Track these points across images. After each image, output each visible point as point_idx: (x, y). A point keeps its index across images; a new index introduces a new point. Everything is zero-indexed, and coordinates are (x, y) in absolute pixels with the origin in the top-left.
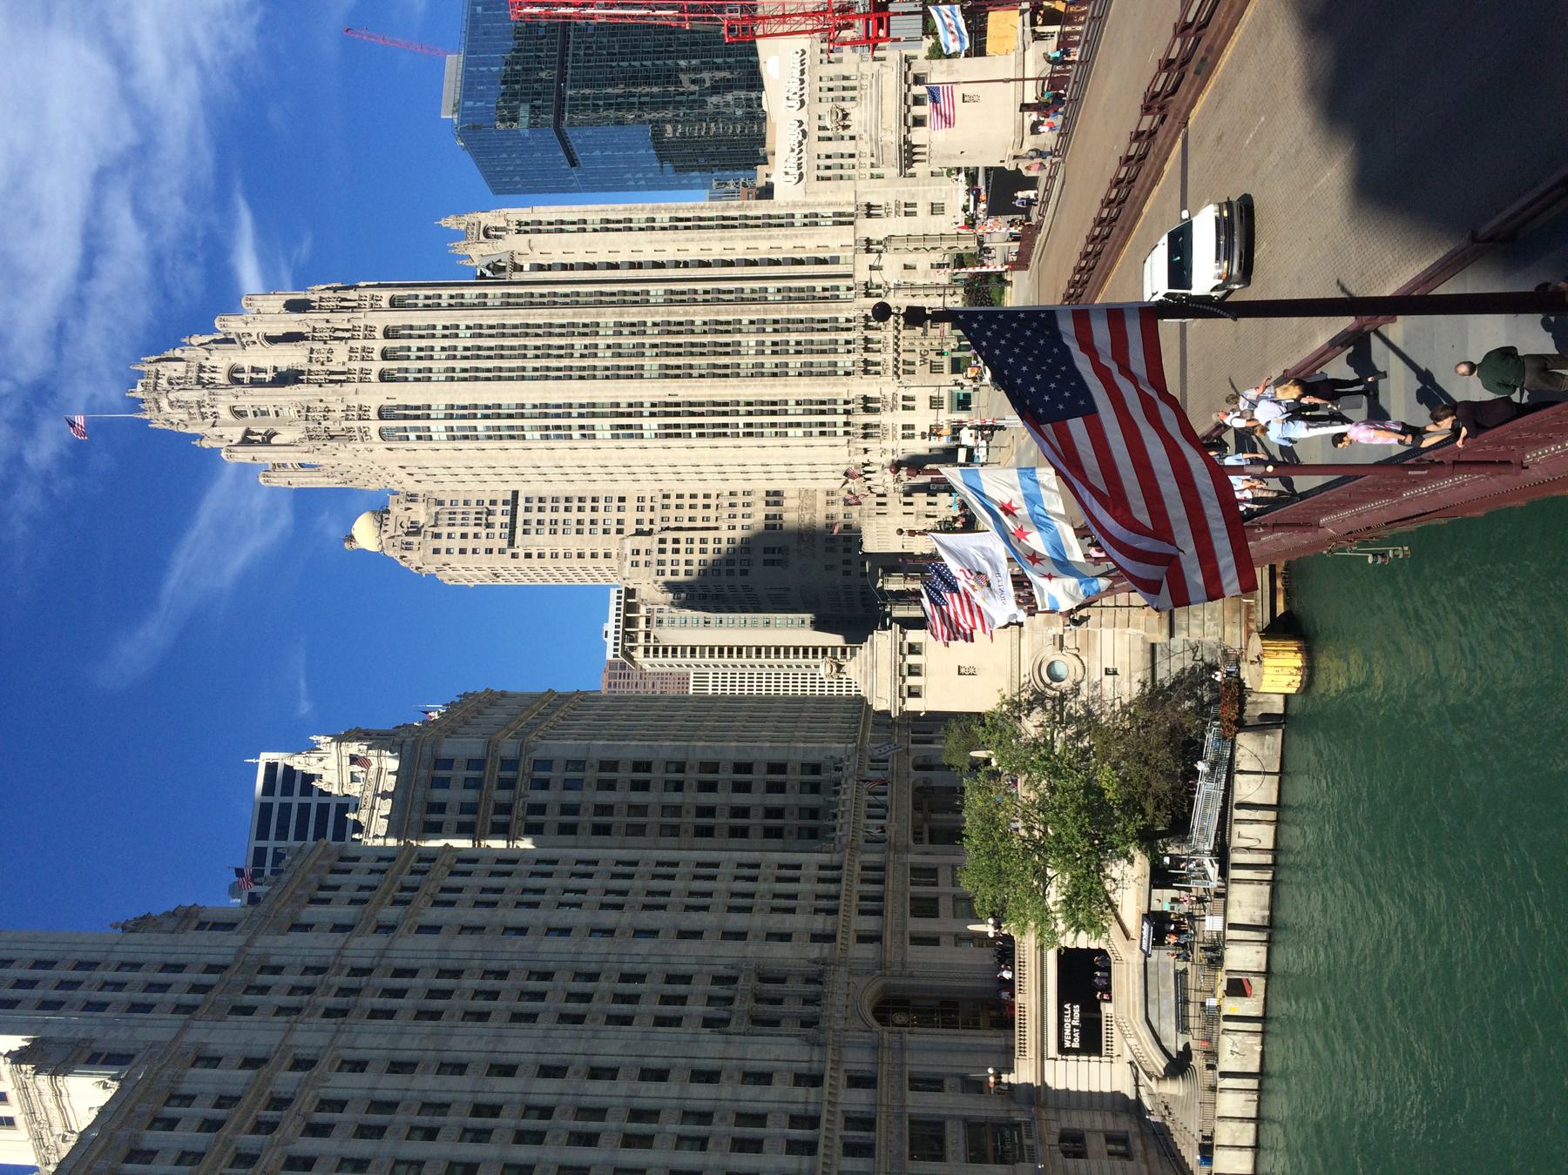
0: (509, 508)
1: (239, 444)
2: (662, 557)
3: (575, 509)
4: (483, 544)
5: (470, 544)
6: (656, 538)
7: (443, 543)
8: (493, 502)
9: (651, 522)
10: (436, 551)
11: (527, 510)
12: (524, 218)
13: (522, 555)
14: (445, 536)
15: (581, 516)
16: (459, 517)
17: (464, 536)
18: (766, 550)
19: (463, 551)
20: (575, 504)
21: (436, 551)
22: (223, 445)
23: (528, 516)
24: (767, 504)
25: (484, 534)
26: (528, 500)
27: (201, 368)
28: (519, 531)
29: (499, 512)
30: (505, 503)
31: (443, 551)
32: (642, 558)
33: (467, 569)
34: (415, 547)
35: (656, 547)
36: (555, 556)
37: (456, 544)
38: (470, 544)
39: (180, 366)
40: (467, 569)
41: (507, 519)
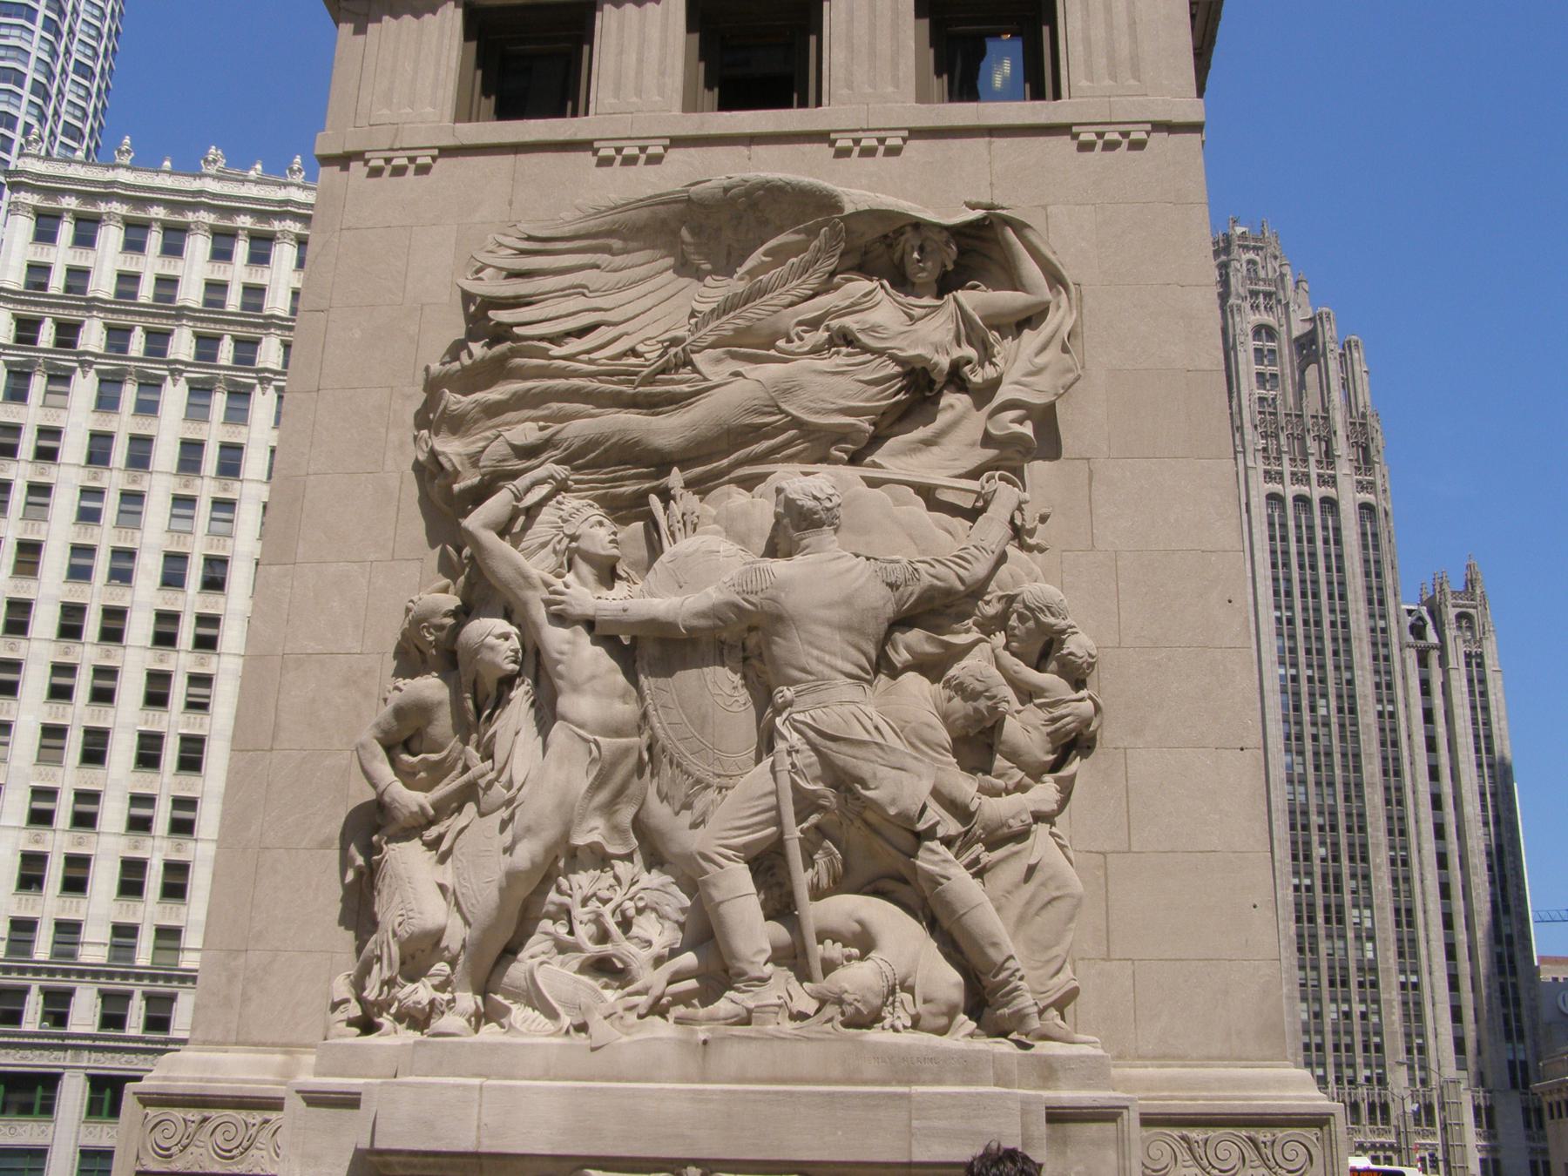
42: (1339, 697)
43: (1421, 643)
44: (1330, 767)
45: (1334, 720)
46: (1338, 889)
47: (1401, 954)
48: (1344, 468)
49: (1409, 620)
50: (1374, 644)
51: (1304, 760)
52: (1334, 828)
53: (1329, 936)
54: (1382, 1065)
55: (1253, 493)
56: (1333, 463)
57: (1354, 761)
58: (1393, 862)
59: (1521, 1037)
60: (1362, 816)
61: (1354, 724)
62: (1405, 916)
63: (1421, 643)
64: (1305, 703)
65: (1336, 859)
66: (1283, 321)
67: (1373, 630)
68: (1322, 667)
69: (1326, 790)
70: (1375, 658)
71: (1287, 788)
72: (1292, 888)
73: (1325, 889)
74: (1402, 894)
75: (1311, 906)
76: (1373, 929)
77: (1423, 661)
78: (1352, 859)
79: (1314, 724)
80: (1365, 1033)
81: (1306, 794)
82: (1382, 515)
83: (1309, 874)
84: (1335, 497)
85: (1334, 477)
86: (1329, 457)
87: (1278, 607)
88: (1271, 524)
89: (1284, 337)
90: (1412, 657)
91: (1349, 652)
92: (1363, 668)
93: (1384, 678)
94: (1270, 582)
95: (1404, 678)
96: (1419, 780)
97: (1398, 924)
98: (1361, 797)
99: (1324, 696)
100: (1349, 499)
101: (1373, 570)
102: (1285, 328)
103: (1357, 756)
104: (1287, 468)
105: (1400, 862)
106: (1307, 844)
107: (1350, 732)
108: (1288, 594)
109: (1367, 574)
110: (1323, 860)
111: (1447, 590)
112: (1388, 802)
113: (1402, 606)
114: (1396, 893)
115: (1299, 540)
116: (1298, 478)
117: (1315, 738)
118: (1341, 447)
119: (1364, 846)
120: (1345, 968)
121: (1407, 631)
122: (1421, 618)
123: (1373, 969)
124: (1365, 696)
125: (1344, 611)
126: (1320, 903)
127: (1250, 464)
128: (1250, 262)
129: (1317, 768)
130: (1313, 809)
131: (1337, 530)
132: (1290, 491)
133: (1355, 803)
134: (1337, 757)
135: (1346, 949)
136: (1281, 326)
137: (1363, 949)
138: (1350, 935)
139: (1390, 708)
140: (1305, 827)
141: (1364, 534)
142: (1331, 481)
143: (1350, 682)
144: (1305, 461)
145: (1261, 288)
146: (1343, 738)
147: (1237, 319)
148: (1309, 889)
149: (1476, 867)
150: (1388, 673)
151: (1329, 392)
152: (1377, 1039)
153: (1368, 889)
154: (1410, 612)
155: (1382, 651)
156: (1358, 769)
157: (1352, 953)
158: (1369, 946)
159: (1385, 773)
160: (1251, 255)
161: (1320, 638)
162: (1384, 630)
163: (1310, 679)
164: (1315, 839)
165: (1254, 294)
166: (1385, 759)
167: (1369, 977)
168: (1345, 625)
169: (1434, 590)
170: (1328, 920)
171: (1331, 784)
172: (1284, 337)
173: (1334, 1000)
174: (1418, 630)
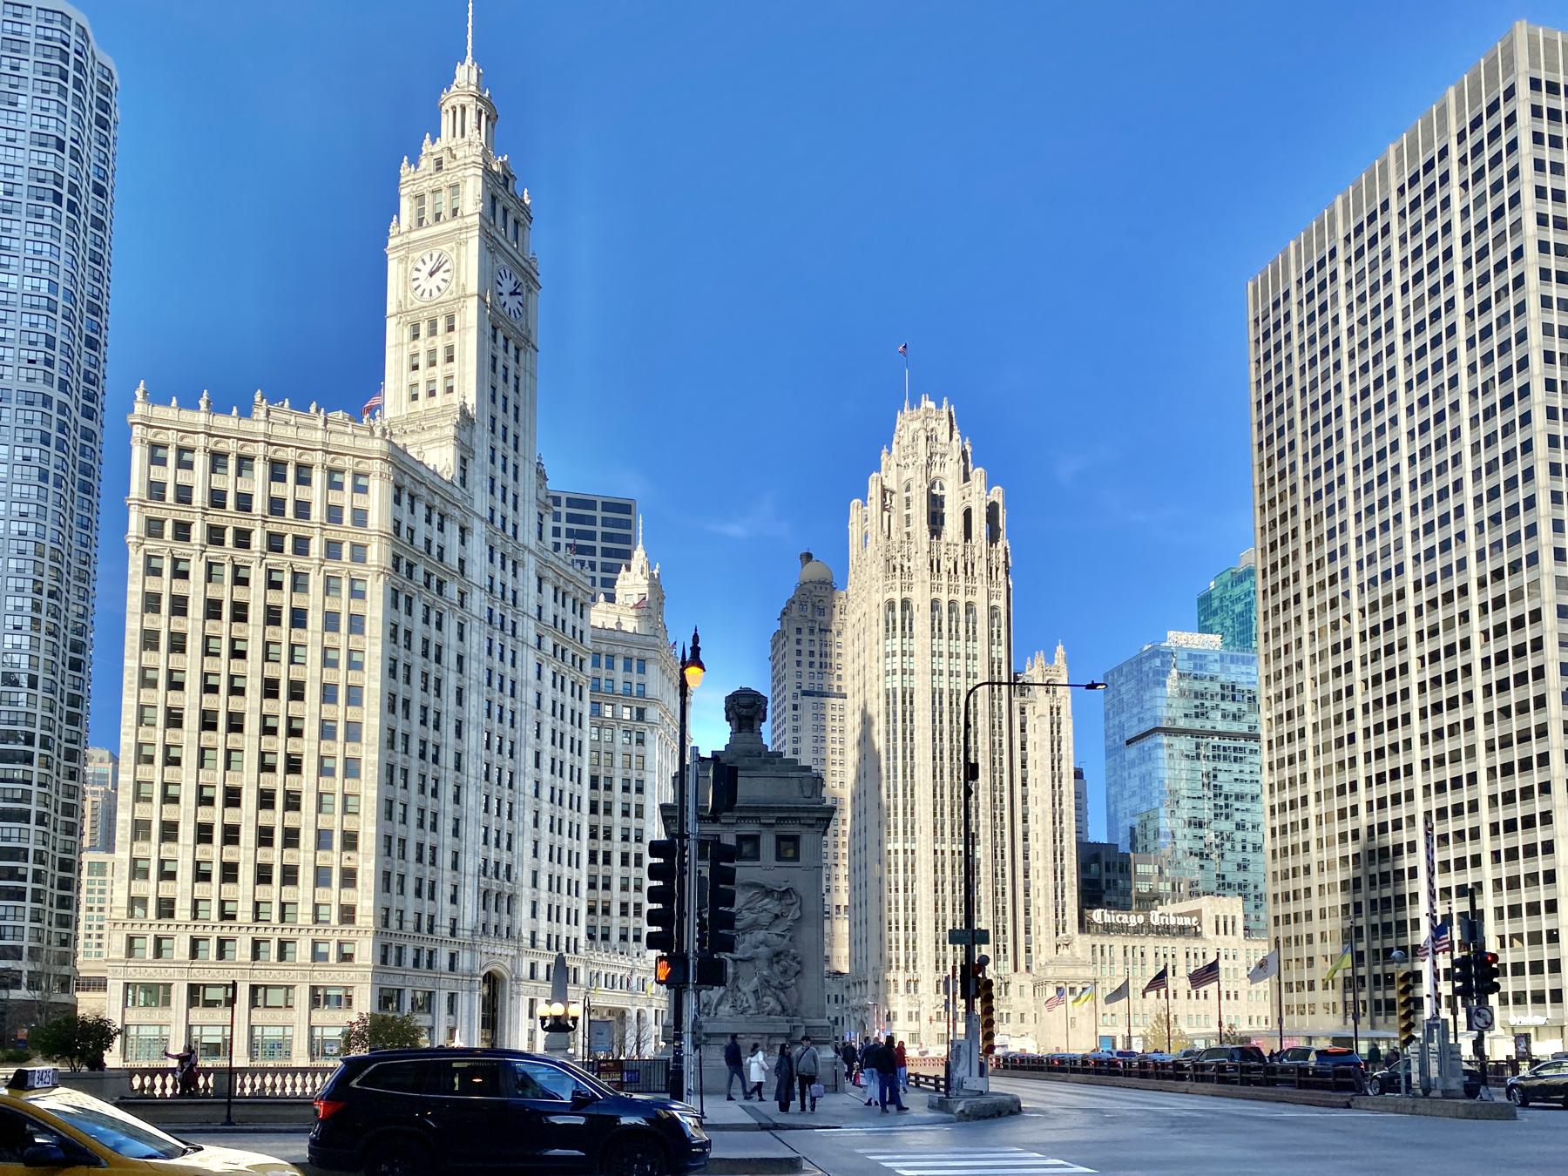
1: (882, 486)
4: (805, 669)
5: (805, 659)
7: (805, 636)
10: (799, 631)
12: (1062, 711)
13: (796, 702)
14: (812, 638)
17: (812, 653)
19: (799, 652)
21: (799, 631)
22: (883, 473)
27: (943, 455)
30: (839, 687)
33: (784, 656)
36: (795, 730)
38: (805, 659)
39: (945, 438)
40: (784, 656)
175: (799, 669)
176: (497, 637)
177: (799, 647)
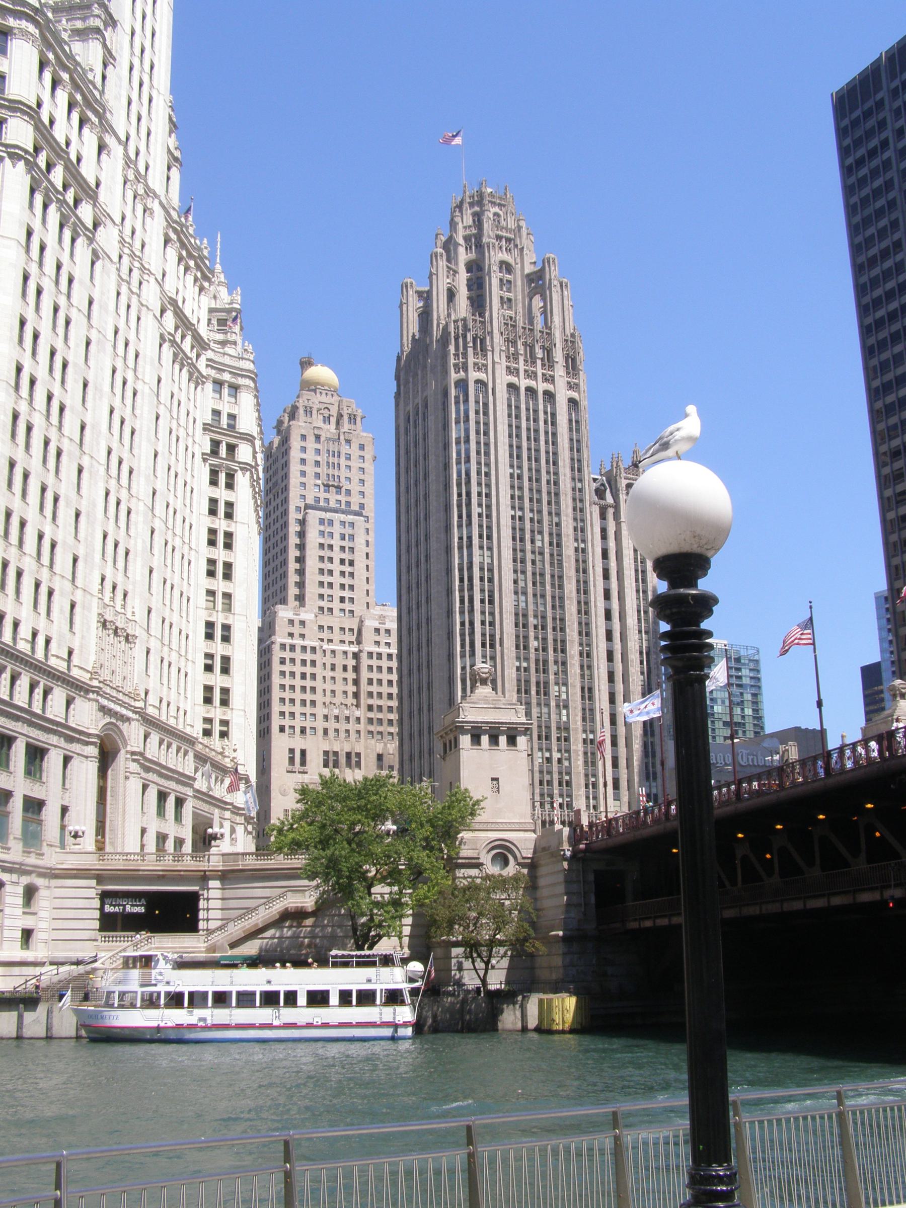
0: (343, 507)
2: (298, 649)
3: (343, 568)
4: (310, 480)
5: (310, 469)
6: (316, 644)
8: (348, 492)
9: (330, 641)
10: (304, 437)
11: (343, 523)
14: (318, 446)
15: (336, 573)
16: (336, 460)
18: (303, 753)
20: (347, 569)
21: (304, 437)
23: (337, 524)
24: (348, 755)
25: (319, 482)
26: (352, 524)
28: (322, 514)
29: (339, 497)
30: (348, 504)
31: (303, 444)
32: (297, 630)
34: (309, 420)
35: (308, 643)
37: (310, 456)
38: (310, 469)
41: (333, 504)
42: (551, 534)
43: (602, 502)
44: (543, 584)
45: (547, 550)
46: (545, 671)
47: (584, 719)
48: (560, 371)
49: (594, 486)
50: (574, 499)
51: (526, 577)
52: (544, 628)
53: (539, 704)
54: (570, 796)
55: (498, 381)
56: (552, 366)
57: (559, 580)
58: (581, 654)
59: (655, 778)
60: (562, 620)
61: (560, 555)
62: (588, 692)
63: (602, 502)
64: (528, 536)
65: (545, 649)
66: (518, 260)
67: (574, 489)
68: (540, 512)
69: (539, 601)
70: (574, 509)
71: (513, 597)
72: (515, 669)
73: (537, 671)
74: (586, 677)
75: (527, 682)
76: (567, 700)
77: (603, 516)
78: (555, 650)
79: (533, 552)
80: (560, 773)
81: (526, 602)
82: (583, 408)
83: (527, 659)
84: (553, 391)
85: (553, 377)
86: (549, 361)
87: (512, 466)
88: (509, 406)
89: (518, 272)
90: (596, 510)
91: (558, 503)
92: (567, 516)
93: (580, 524)
94: (507, 447)
95: (592, 525)
96: (598, 598)
97: (583, 698)
98: (562, 607)
99: (541, 532)
100: (562, 395)
101: (576, 446)
102: (519, 266)
103: (561, 577)
104: (522, 366)
105: (586, 655)
106: (526, 638)
107: (557, 561)
108: (519, 457)
109: (571, 449)
110: (536, 650)
111: (622, 467)
112: (579, 612)
113: (591, 474)
114: (582, 676)
115: (528, 419)
116: (532, 375)
117: (534, 562)
118: (559, 355)
119: (563, 642)
120: (548, 727)
121: (593, 493)
122: (603, 485)
123: (567, 729)
124: (568, 535)
125: (556, 474)
126: (533, 680)
127: (497, 359)
128: (496, 214)
129: (534, 584)
130: (531, 613)
131: (554, 415)
132: (524, 383)
133: (558, 611)
134: (548, 577)
135: (549, 714)
136: (516, 264)
137: (560, 714)
138: (553, 703)
139: (582, 546)
140: (525, 626)
141: (570, 421)
142: (550, 379)
143: (558, 525)
144: (534, 363)
145: (504, 234)
146: (552, 564)
147: (492, 253)
148: (526, 669)
149: (632, 661)
150: (582, 520)
151: (552, 315)
152: (567, 778)
153: (565, 672)
154: (595, 480)
155: (579, 505)
156: (561, 587)
157: (554, 717)
158: (564, 712)
159: (578, 591)
160: (496, 209)
161: (539, 491)
162: (580, 490)
163: (532, 520)
164: (532, 634)
165: (499, 238)
166: (578, 581)
167: (564, 734)
168: (556, 483)
169: (612, 466)
170: (538, 693)
171: (543, 596)
172: (518, 272)
173: (540, 749)
174: (600, 493)
175: (303, 480)
176: (124, 289)
177: (304, 456)
